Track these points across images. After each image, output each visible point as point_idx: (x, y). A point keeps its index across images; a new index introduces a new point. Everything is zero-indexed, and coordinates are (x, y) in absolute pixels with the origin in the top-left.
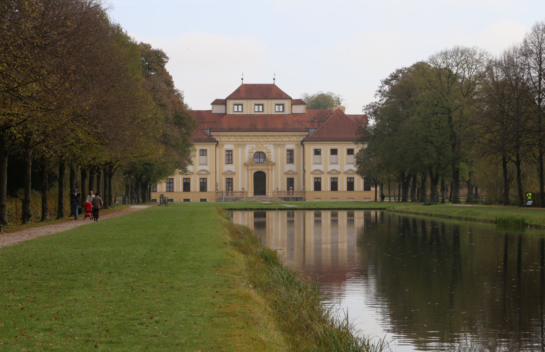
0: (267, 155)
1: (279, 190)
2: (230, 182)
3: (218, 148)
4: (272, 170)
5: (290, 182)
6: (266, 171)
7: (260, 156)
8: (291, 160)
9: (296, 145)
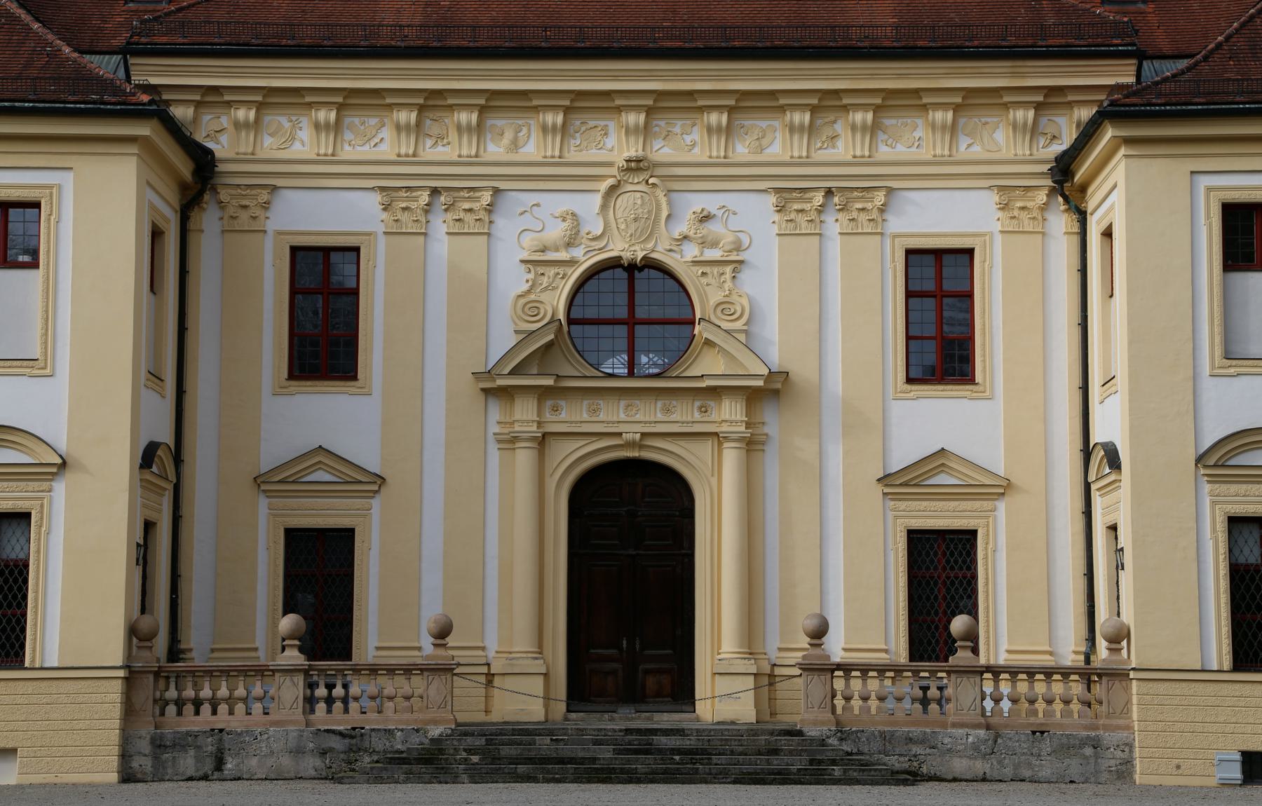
0: (706, 295)
1: (836, 647)
2: (320, 572)
3: (208, 220)
4: (752, 445)
5: (941, 573)
6: (690, 461)
7: (629, 311)
8: (942, 347)
9: (1009, 193)
